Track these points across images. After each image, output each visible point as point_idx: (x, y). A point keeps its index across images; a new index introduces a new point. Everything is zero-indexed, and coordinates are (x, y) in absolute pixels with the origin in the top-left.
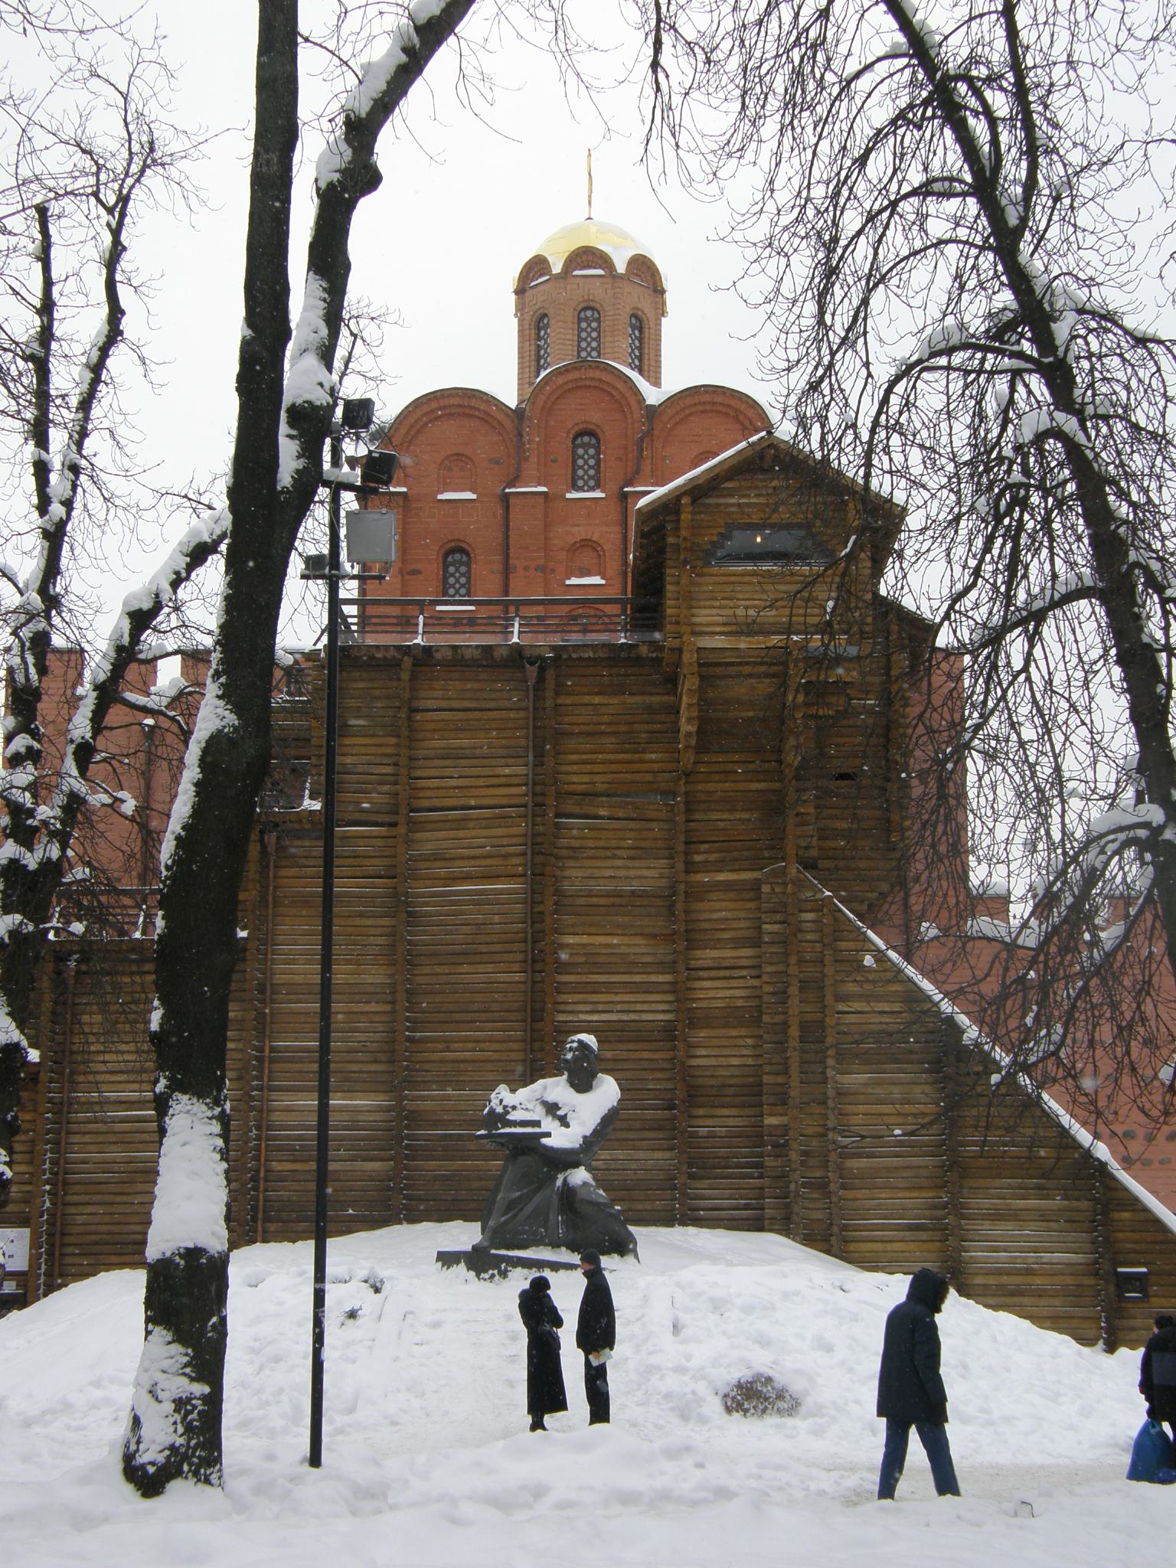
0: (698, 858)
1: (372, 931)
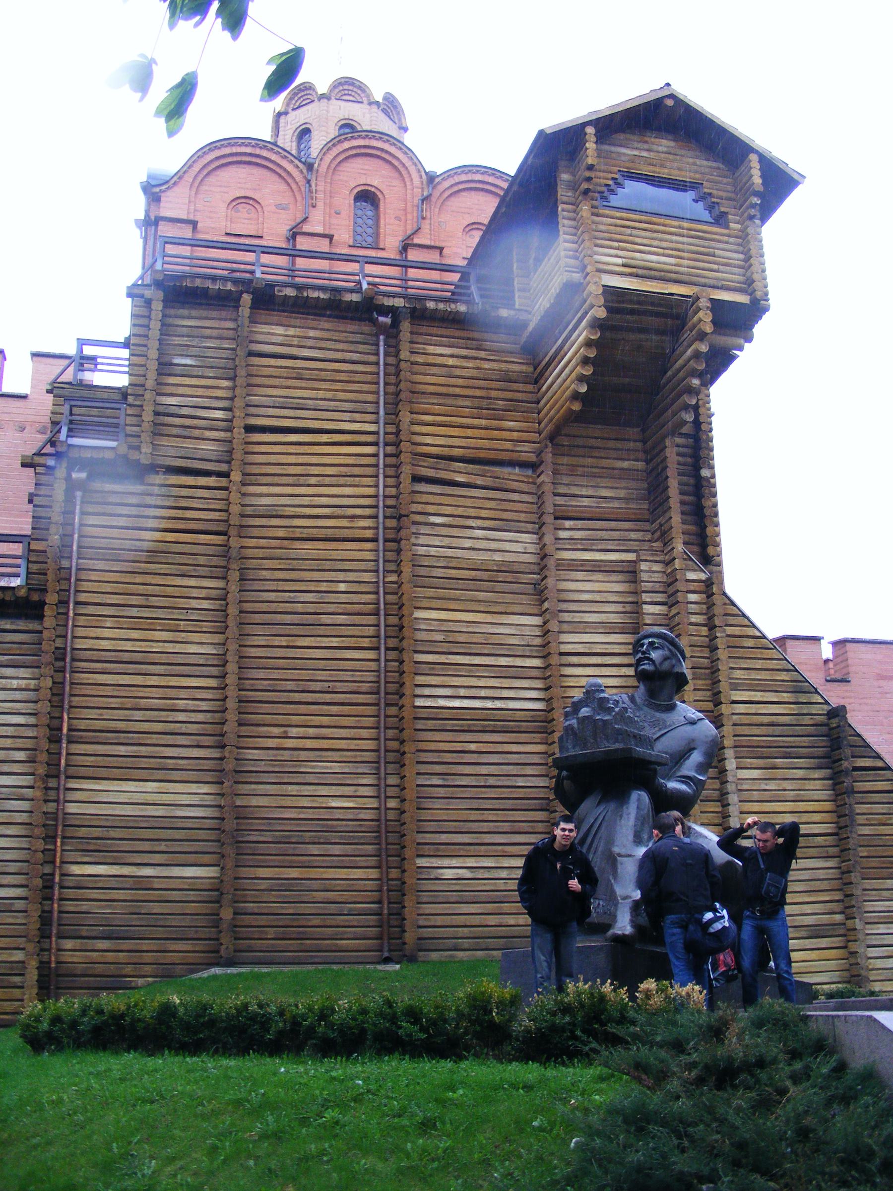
0: (563, 534)
1: (195, 593)
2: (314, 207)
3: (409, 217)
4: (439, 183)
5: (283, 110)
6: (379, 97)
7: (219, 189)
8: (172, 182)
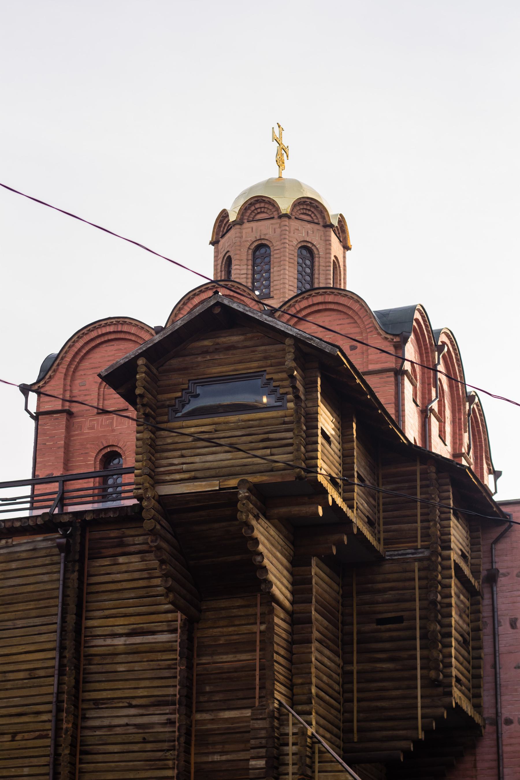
5: (214, 240)
8: (47, 377)
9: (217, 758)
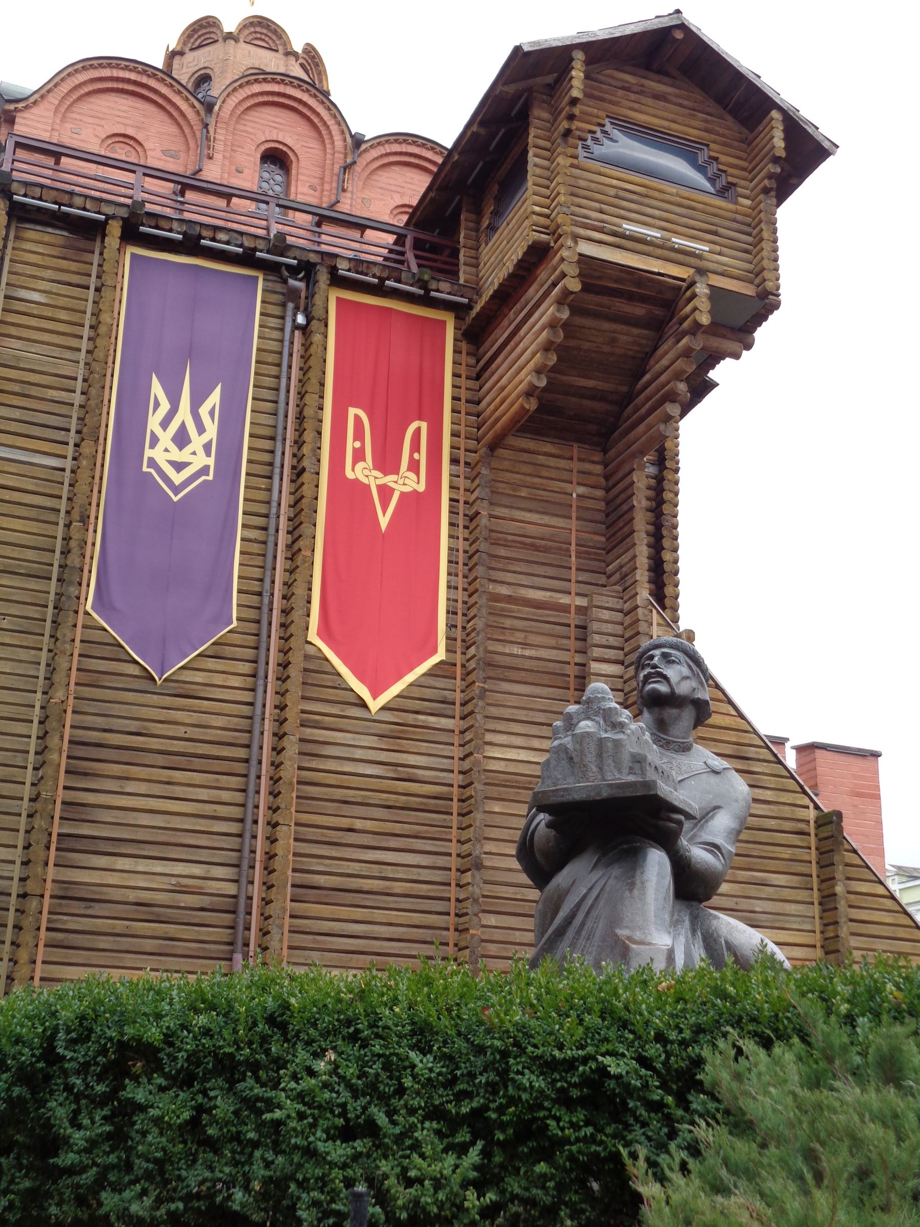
2: (211, 158)
3: (327, 187)
4: (365, 150)
5: (178, 49)
6: (298, 47)
7: (91, 120)
8: (32, 100)
9: (516, 650)
